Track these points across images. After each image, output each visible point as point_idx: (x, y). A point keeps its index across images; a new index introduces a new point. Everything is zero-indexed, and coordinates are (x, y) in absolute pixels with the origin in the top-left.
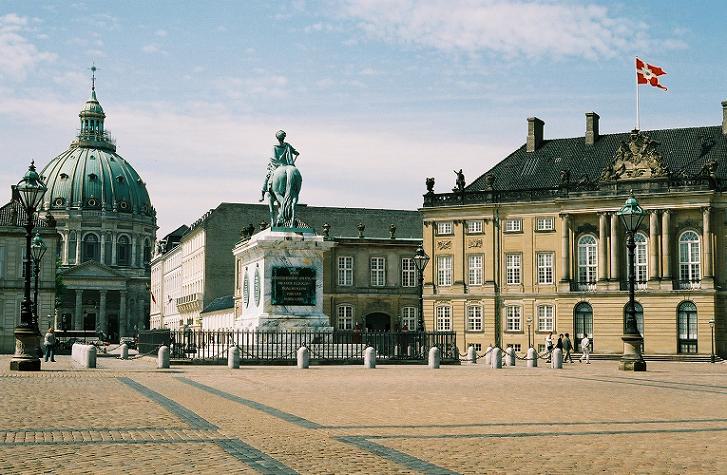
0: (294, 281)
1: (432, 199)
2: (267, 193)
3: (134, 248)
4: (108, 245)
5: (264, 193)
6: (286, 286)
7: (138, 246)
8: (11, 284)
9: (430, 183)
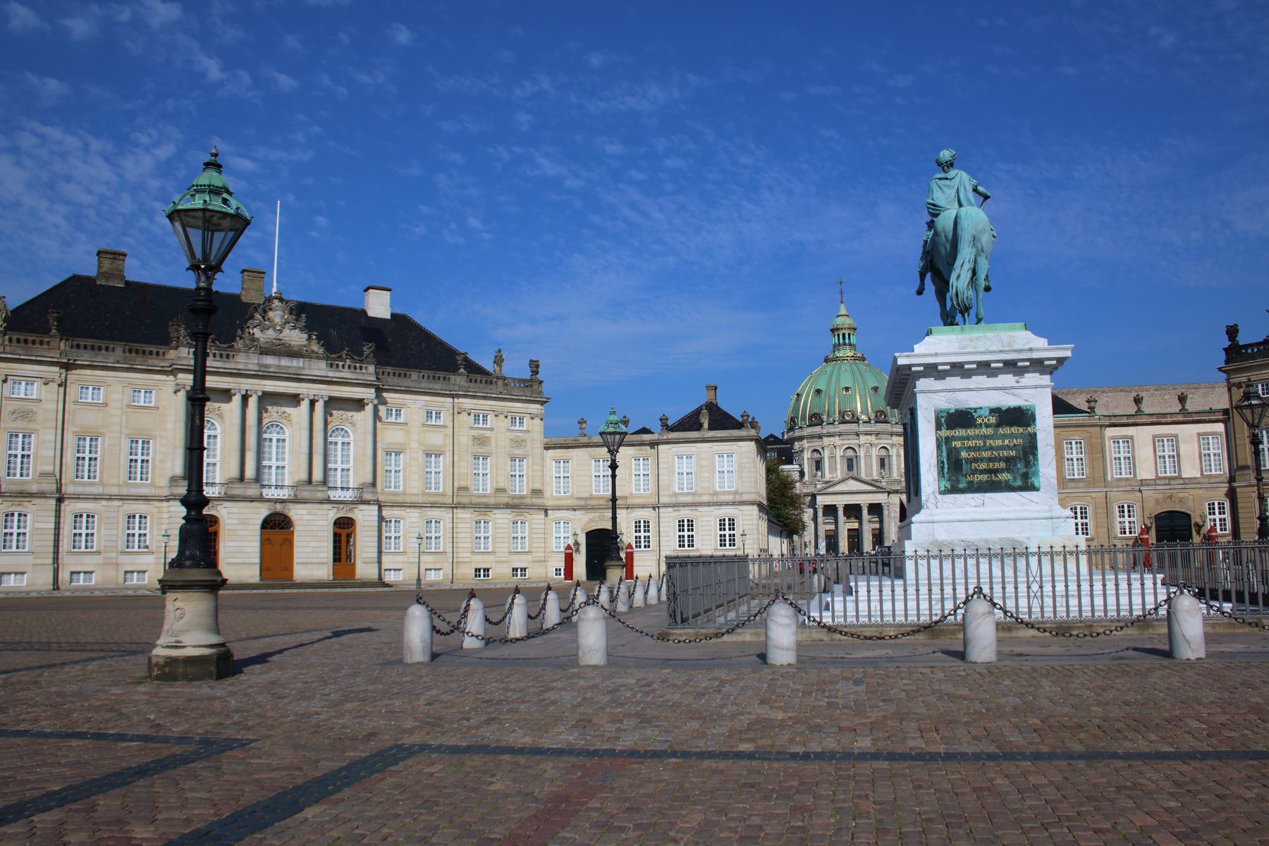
0: (986, 437)
1: (1236, 353)
2: (929, 275)
3: (894, 458)
4: (868, 457)
5: (922, 276)
6: (969, 449)
7: (898, 456)
8: (705, 499)
9: (1232, 332)
